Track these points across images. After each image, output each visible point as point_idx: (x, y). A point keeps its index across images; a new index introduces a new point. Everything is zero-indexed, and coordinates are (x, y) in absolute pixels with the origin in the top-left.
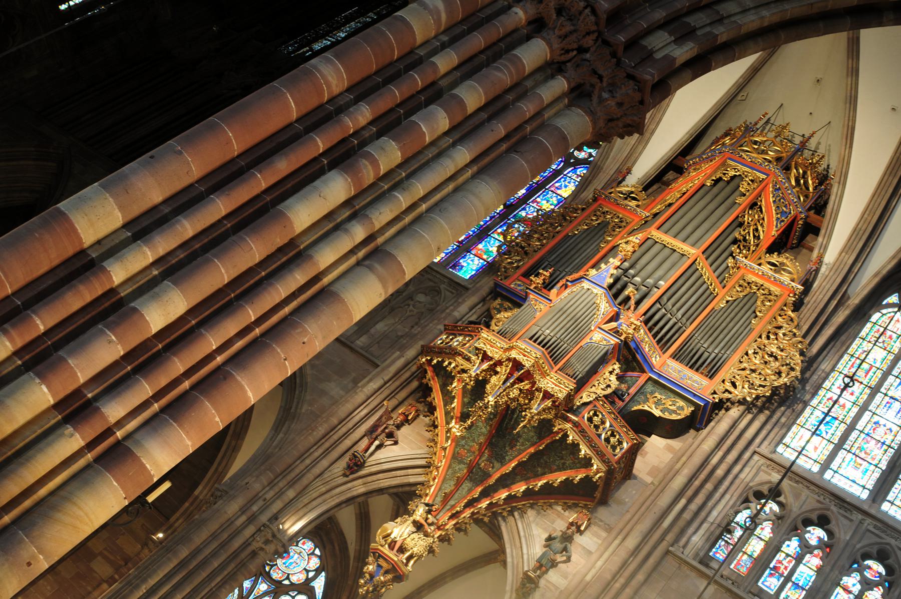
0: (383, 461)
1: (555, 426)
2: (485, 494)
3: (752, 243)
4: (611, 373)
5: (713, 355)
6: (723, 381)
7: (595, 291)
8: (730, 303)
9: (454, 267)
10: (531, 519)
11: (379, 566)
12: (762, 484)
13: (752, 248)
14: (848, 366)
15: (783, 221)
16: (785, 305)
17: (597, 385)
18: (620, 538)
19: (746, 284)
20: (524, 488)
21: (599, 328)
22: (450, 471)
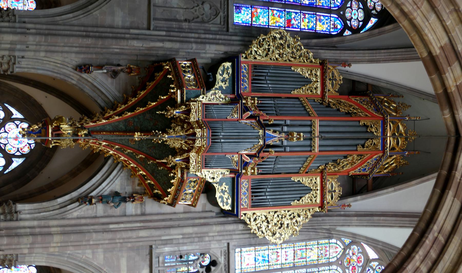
1: (175, 170)
9: (238, 8)
17: (210, 172)
21: (241, 156)
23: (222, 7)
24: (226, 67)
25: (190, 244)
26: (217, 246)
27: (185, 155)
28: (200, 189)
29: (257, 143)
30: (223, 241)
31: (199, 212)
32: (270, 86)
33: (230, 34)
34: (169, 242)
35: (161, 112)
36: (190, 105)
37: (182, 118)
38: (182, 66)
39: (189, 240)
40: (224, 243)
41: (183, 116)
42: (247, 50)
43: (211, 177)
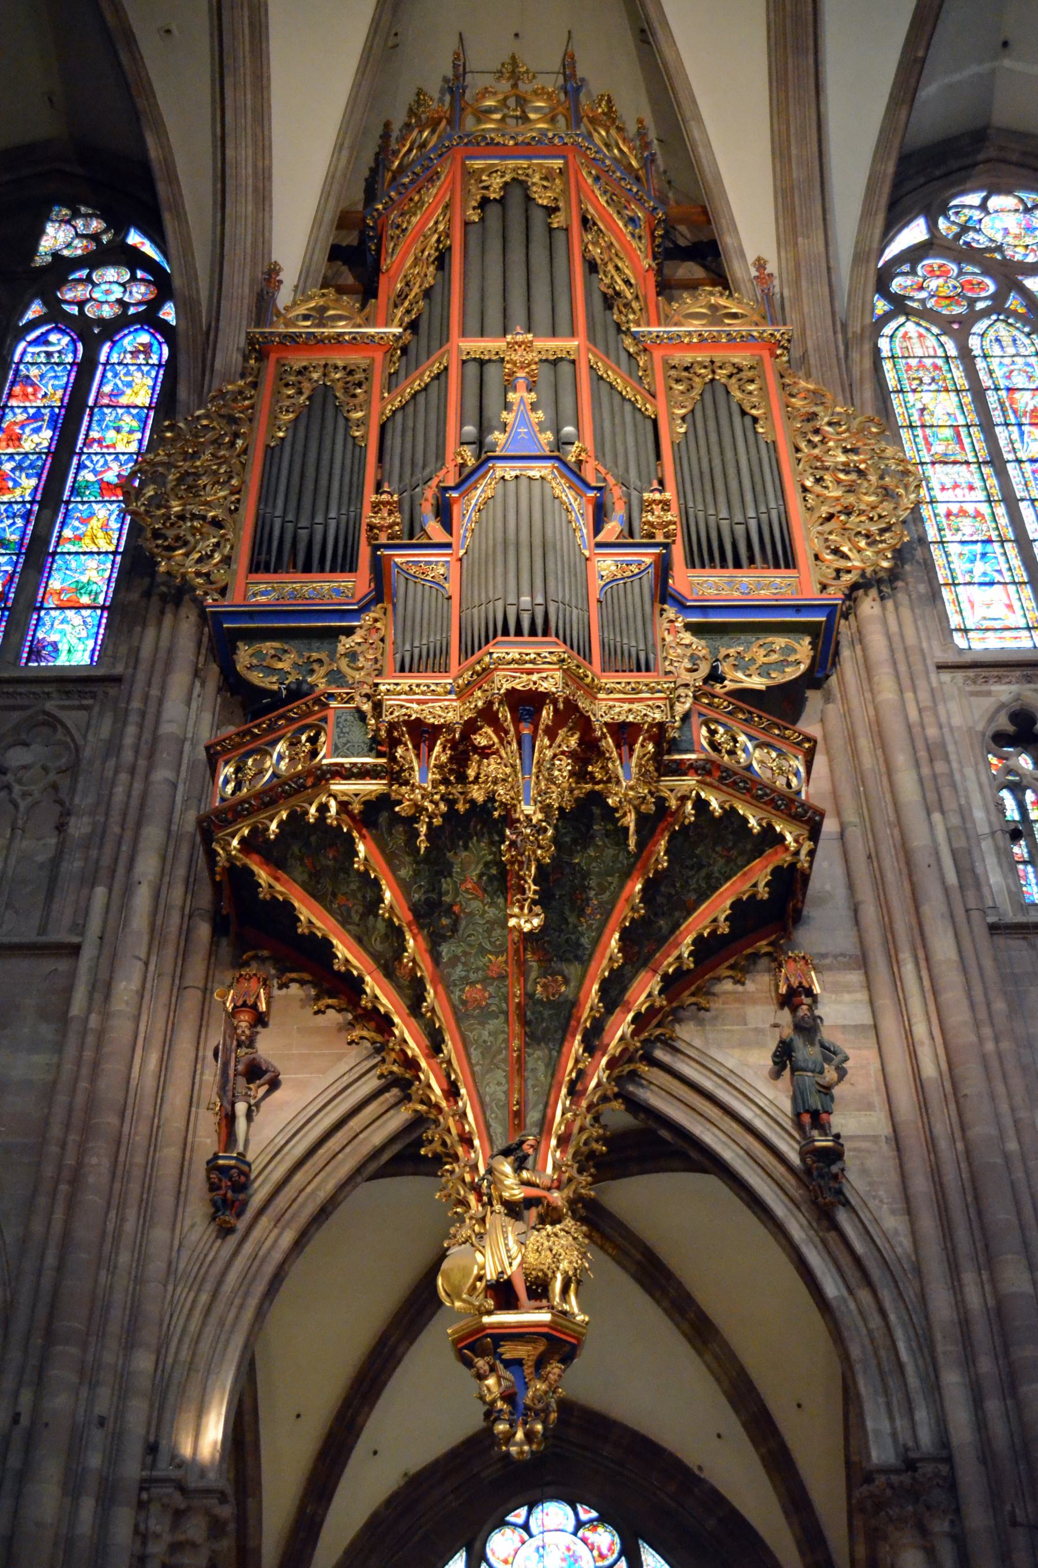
0: (280, 1141)
3: (629, 296)
5: (753, 524)
6: (817, 557)
7: (535, 474)
8: (689, 418)
9: (35, 653)
10: (697, 1042)
12: (992, 719)
13: (635, 305)
14: (922, 445)
15: (640, 238)
16: (782, 377)
18: (906, 956)
19: (686, 374)
20: (655, 984)
21: (599, 545)
22: (475, 1054)
23: (26, 702)
24: (255, 662)
25: (962, 793)
26: (953, 706)
29: (547, 486)
30: (935, 684)
32: (333, 514)
33: (130, 670)
35: (422, 838)
36: (390, 723)
37: (444, 758)
38: (233, 793)
39: (946, 792)
40: (941, 683)
41: (439, 753)
42: (193, 589)
43: (689, 666)
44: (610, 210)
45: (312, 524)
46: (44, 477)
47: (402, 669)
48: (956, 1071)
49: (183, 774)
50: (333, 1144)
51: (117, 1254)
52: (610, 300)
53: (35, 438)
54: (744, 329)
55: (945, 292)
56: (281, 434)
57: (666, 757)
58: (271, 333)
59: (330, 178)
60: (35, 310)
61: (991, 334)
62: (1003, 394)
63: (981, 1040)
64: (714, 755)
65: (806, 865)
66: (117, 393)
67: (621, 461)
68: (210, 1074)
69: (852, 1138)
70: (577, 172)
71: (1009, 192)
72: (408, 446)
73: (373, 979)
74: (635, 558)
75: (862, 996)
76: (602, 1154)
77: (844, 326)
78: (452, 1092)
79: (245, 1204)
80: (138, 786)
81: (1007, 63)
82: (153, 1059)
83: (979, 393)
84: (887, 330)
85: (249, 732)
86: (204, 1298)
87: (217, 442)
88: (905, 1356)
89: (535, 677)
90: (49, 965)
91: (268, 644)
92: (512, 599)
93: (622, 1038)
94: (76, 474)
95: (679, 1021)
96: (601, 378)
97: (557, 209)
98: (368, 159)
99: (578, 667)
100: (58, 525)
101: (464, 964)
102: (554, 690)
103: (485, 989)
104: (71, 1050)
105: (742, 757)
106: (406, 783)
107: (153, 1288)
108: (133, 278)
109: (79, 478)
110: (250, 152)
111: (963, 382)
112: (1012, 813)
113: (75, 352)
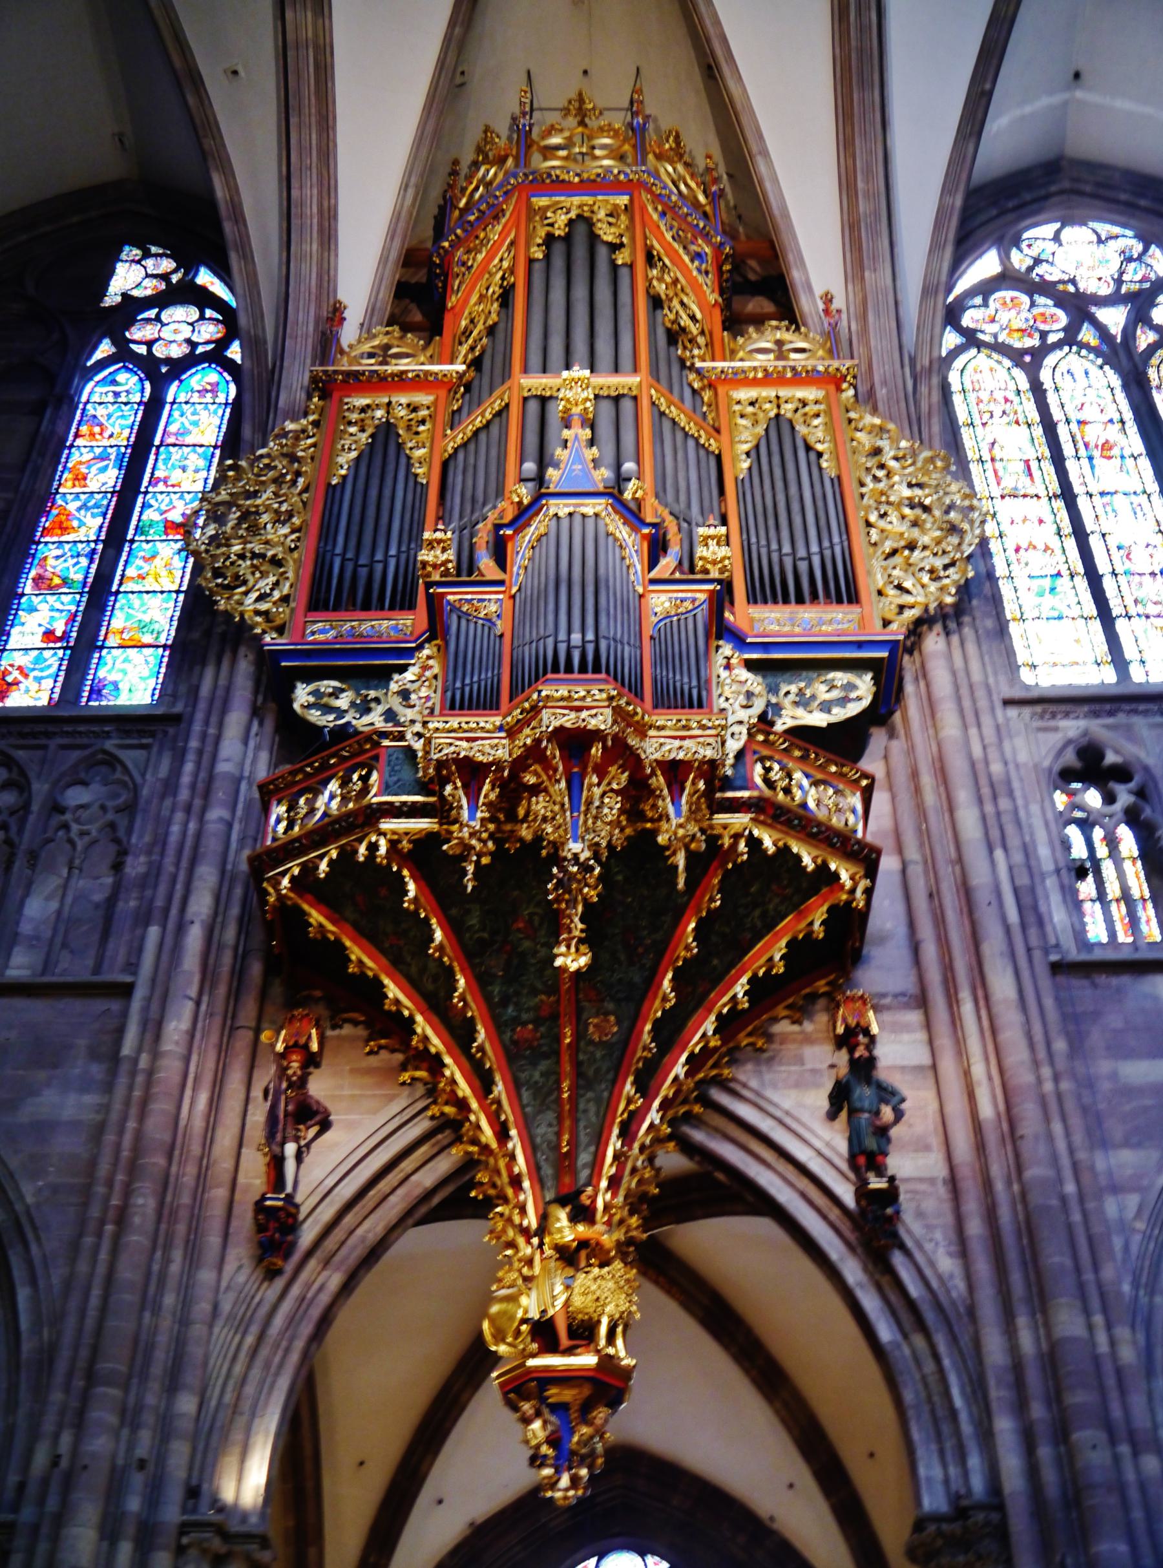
0: (330, 1182)
1: (720, 837)
2: (645, 1088)
4: (728, 667)
5: (816, 560)
7: (589, 511)
9: (96, 692)
10: (753, 1083)
11: (559, 1408)
13: (701, 340)
15: (707, 273)
16: (847, 411)
18: (965, 995)
19: (750, 409)
20: (709, 1025)
21: (653, 582)
23: (85, 741)
24: (312, 699)
25: (1026, 830)
26: (1019, 742)
27: (658, 781)
28: (797, 753)
29: (601, 523)
30: (1000, 720)
31: (893, 798)
32: (393, 551)
33: (189, 709)
34: (1027, 900)
35: (470, 876)
37: (492, 796)
38: (285, 833)
39: (1010, 829)
40: (1008, 720)
41: (488, 791)
42: (252, 627)
44: (675, 245)
45: (373, 562)
46: (109, 516)
47: (452, 707)
48: (1015, 1111)
49: (239, 812)
50: (384, 1186)
51: (162, 1296)
52: (675, 336)
53: (102, 478)
54: (810, 364)
55: (1018, 324)
56: (343, 472)
57: (718, 795)
58: (335, 372)
59: (396, 217)
60: (105, 348)
61: (1063, 367)
62: (1074, 426)
63: (1039, 1081)
64: (767, 793)
65: (861, 904)
66: (186, 432)
67: (683, 497)
68: (258, 1115)
69: (907, 1180)
70: (643, 209)
71: (1083, 223)
72: (470, 483)
73: (426, 1019)
74: (689, 595)
75: (922, 1036)
76: (655, 1197)
77: (913, 360)
78: (502, 1134)
79: (292, 1246)
80: (192, 826)
81: (1079, 94)
82: (203, 1098)
83: (1049, 427)
84: (958, 363)
85: (302, 770)
86: (250, 1340)
87: (278, 481)
88: (958, 1402)
89: (584, 714)
90: (99, 1005)
91: (326, 682)
92: (562, 636)
93: (676, 1078)
94: (141, 513)
95: (733, 1062)
96: (662, 414)
97: (622, 245)
98: (435, 194)
99: (628, 704)
100: (122, 563)
101: (516, 1004)
102: (603, 727)
103: (535, 1030)
104: (120, 1091)
105: (798, 795)
106: (456, 821)
107: (197, 1330)
108: (202, 317)
109: (144, 517)
110: (315, 192)
111: (1035, 416)
112: (1079, 851)
113: (143, 390)
